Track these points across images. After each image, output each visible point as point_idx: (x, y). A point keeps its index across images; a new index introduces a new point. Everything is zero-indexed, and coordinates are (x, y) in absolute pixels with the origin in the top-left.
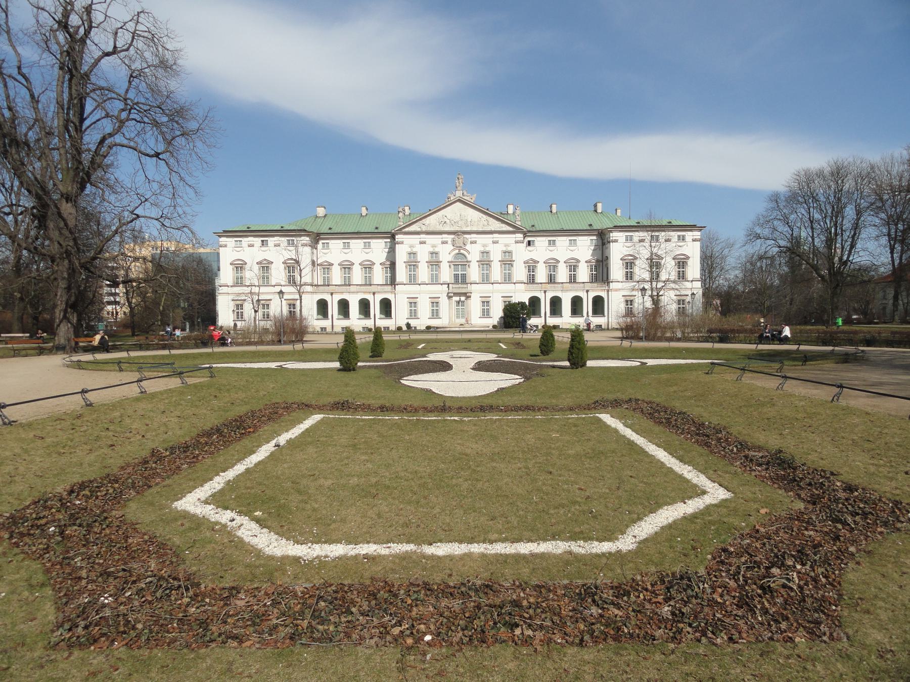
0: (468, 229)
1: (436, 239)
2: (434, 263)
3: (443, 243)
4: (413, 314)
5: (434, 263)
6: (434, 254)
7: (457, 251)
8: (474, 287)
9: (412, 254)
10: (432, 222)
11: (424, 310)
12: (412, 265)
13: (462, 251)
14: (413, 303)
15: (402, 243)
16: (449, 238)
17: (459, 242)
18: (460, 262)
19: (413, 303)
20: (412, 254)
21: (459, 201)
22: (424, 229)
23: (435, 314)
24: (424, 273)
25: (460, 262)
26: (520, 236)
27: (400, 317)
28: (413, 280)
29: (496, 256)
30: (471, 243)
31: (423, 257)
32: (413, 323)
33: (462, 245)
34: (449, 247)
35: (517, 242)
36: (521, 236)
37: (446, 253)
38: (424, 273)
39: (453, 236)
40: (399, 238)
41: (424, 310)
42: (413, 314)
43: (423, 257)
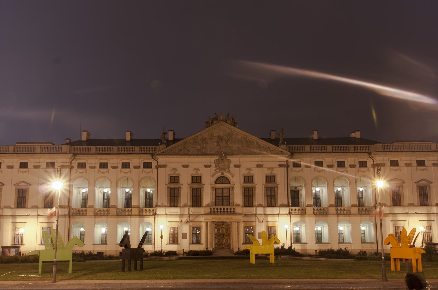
3: (206, 166)
7: (219, 174)
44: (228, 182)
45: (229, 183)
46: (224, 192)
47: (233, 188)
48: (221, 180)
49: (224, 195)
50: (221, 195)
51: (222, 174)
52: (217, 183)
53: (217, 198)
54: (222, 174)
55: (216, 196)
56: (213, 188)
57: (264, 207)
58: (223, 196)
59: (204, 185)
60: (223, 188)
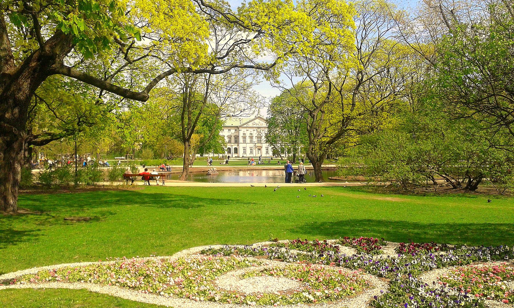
1: (251, 130)
2: (251, 137)
4: (245, 152)
5: (251, 137)
10: (250, 124)
11: (248, 151)
12: (244, 138)
14: (245, 149)
17: (259, 130)
19: (245, 149)
23: (251, 152)
24: (248, 140)
27: (241, 153)
28: (245, 142)
31: (248, 135)
32: (245, 155)
34: (256, 132)
37: (255, 134)
38: (248, 140)
40: (240, 129)
41: (248, 151)
42: (245, 152)
43: (248, 135)
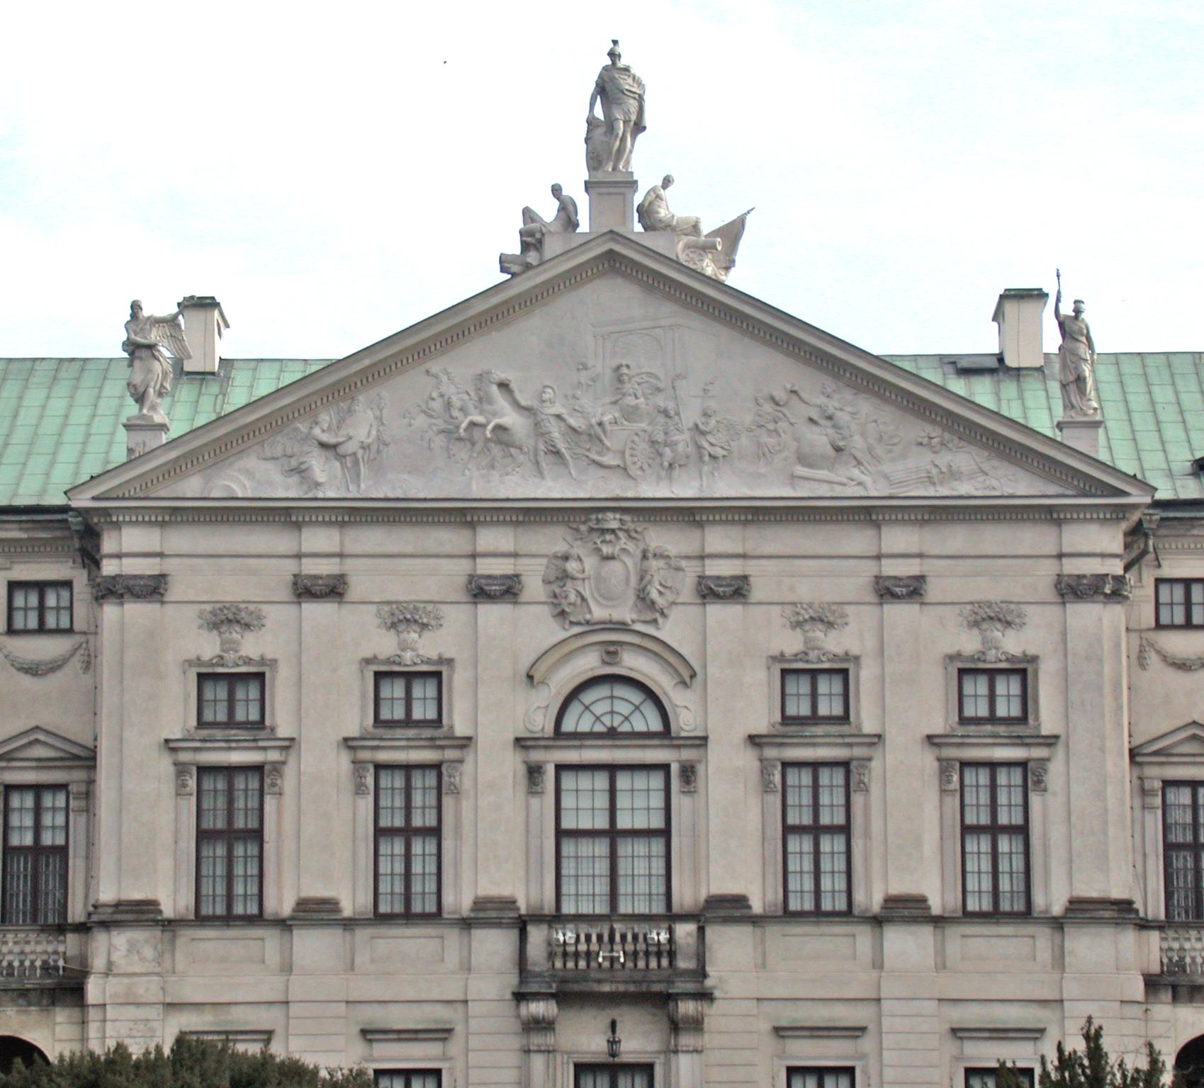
0: (685, 488)
1: (425, 569)
3: (482, 592)
6: (407, 689)
7: (589, 664)
8: (730, 950)
9: (232, 691)
13: (634, 664)
15: (152, 589)
16: (528, 554)
18: (616, 742)
20: (232, 691)
21: (614, 261)
22: (330, 481)
25: (616, 742)
26: (1097, 547)
29: (904, 705)
30: (709, 592)
33: (625, 612)
35: (1073, 590)
36: (1111, 539)
39: (553, 540)
40: (128, 549)
44: (656, 725)
45: (666, 734)
46: (622, 801)
47: (688, 773)
48: (599, 709)
49: (623, 822)
50: (602, 823)
51: (611, 652)
52: (568, 726)
53: (568, 847)
54: (611, 652)
55: (561, 834)
56: (534, 772)
57: (939, 921)
58: (613, 834)
59: (466, 743)
60: (612, 769)
